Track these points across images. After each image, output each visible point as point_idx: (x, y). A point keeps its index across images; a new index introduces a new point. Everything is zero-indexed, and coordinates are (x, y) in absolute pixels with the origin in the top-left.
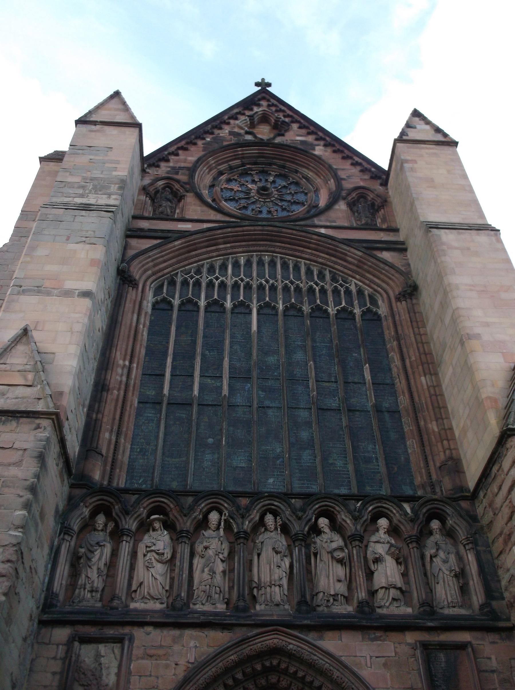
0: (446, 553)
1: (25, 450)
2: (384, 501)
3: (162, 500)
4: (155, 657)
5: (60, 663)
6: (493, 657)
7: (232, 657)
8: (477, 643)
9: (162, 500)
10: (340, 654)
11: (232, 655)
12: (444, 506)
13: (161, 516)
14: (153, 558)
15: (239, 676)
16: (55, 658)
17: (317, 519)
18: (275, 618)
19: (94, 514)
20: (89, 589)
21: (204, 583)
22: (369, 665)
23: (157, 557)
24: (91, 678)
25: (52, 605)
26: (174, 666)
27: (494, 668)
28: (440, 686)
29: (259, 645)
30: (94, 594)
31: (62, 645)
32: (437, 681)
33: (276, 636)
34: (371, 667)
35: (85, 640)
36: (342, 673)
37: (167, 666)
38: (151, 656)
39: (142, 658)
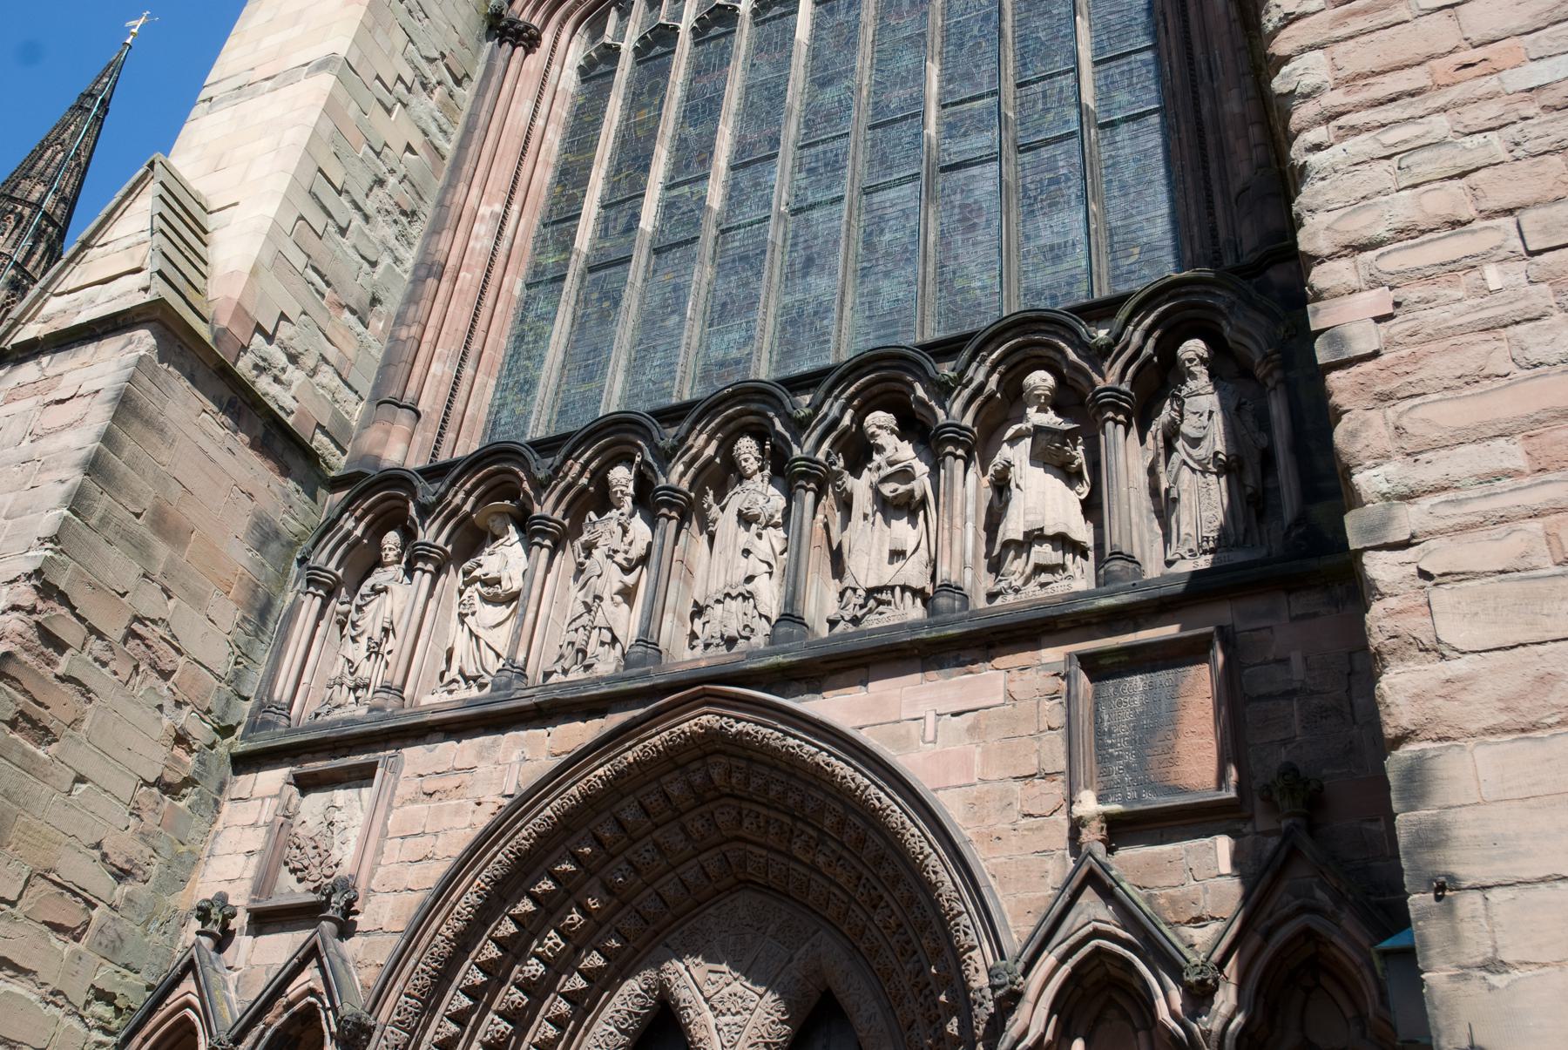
0: (1206, 415)
1: (97, 392)
2: (1035, 327)
3: (506, 465)
4: (437, 795)
5: (262, 832)
6: (1296, 658)
7: (600, 772)
8: (1253, 625)
9: (506, 465)
10: (859, 724)
11: (601, 765)
12: (1207, 293)
13: (507, 502)
14: (476, 595)
15: (630, 814)
16: (254, 825)
17: (859, 419)
18: (703, 664)
19: (376, 532)
20: (352, 685)
21: (573, 626)
22: (930, 736)
23: (484, 590)
24: (312, 853)
25: (266, 724)
26: (473, 806)
27: (1298, 685)
28: (1119, 757)
29: (665, 734)
30: (359, 693)
31: (271, 797)
32: (1112, 746)
33: (705, 709)
34: (934, 742)
35: (305, 784)
36: (856, 769)
37: (458, 811)
38: (431, 795)
39: (413, 801)
